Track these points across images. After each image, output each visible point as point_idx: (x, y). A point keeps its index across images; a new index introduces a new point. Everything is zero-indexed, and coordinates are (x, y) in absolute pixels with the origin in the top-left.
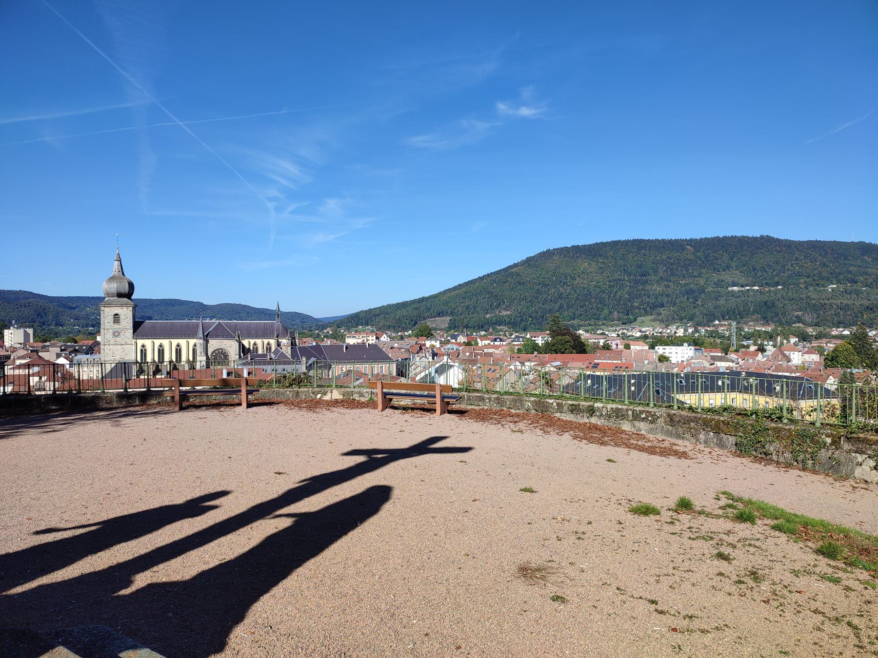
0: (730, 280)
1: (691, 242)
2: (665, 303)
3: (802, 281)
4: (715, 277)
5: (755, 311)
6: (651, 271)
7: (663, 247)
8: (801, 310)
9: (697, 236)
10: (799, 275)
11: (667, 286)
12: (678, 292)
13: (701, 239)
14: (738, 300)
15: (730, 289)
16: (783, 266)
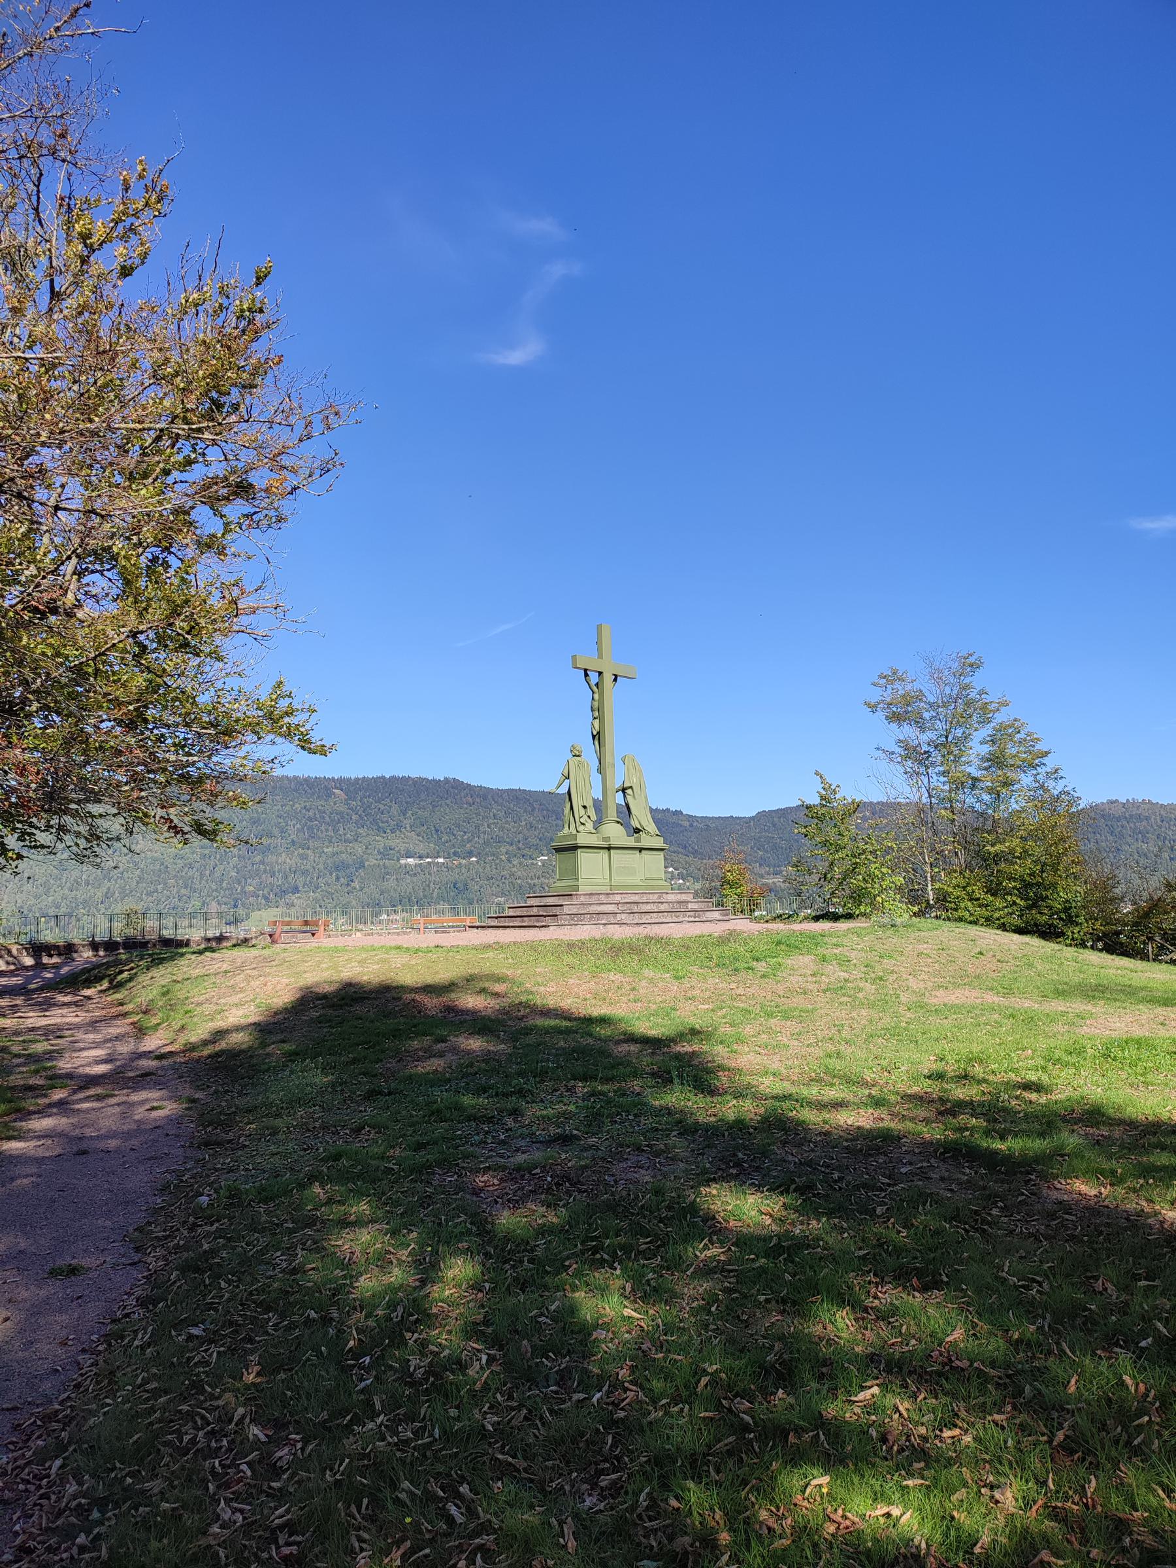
0: (402, 847)
1: (341, 783)
2: (300, 885)
3: (503, 850)
4: (381, 842)
5: (441, 898)
6: (276, 831)
7: (296, 790)
8: (503, 894)
9: (352, 775)
10: (499, 840)
11: (303, 857)
12: (321, 866)
13: (357, 779)
14: (415, 879)
15: (403, 862)
16: (477, 827)
